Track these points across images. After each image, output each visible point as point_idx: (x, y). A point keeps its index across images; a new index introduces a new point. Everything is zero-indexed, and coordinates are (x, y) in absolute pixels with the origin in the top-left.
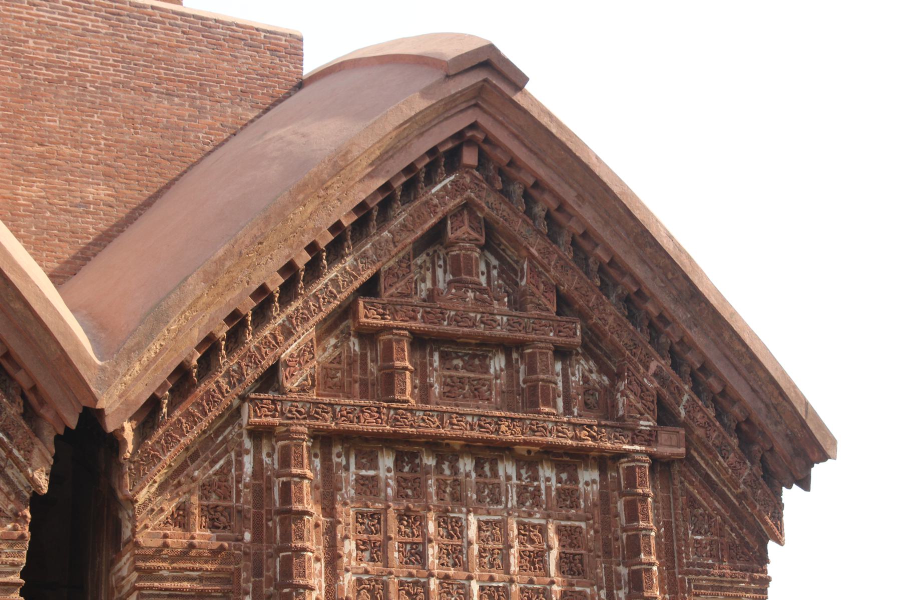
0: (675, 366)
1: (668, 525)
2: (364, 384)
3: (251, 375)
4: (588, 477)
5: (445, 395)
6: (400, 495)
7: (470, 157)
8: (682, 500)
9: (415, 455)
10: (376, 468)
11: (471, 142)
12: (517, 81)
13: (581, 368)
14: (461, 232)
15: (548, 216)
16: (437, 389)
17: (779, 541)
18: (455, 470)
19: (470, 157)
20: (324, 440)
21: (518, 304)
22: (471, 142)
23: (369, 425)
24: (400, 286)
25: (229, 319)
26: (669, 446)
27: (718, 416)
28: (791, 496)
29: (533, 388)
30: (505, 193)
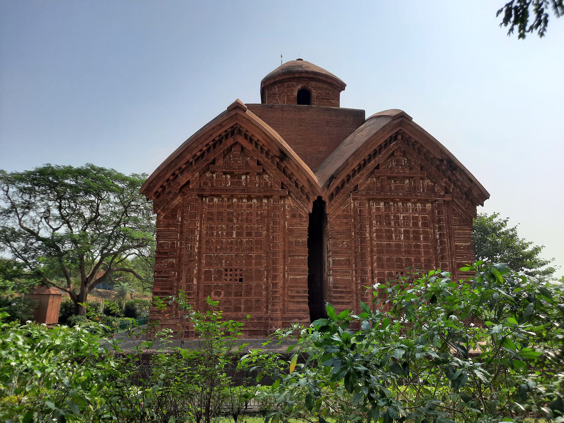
0: (449, 180)
1: (448, 216)
2: (377, 188)
4: (429, 205)
5: (395, 189)
6: (385, 211)
7: (399, 137)
8: (451, 209)
9: (388, 202)
11: (400, 134)
12: (410, 119)
13: (427, 182)
15: (418, 148)
18: (397, 205)
21: (411, 169)
22: (400, 134)
24: (384, 167)
25: (347, 176)
26: (448, 198)
27: (460, 191)
29: (415, 187)
30: (408, 144)
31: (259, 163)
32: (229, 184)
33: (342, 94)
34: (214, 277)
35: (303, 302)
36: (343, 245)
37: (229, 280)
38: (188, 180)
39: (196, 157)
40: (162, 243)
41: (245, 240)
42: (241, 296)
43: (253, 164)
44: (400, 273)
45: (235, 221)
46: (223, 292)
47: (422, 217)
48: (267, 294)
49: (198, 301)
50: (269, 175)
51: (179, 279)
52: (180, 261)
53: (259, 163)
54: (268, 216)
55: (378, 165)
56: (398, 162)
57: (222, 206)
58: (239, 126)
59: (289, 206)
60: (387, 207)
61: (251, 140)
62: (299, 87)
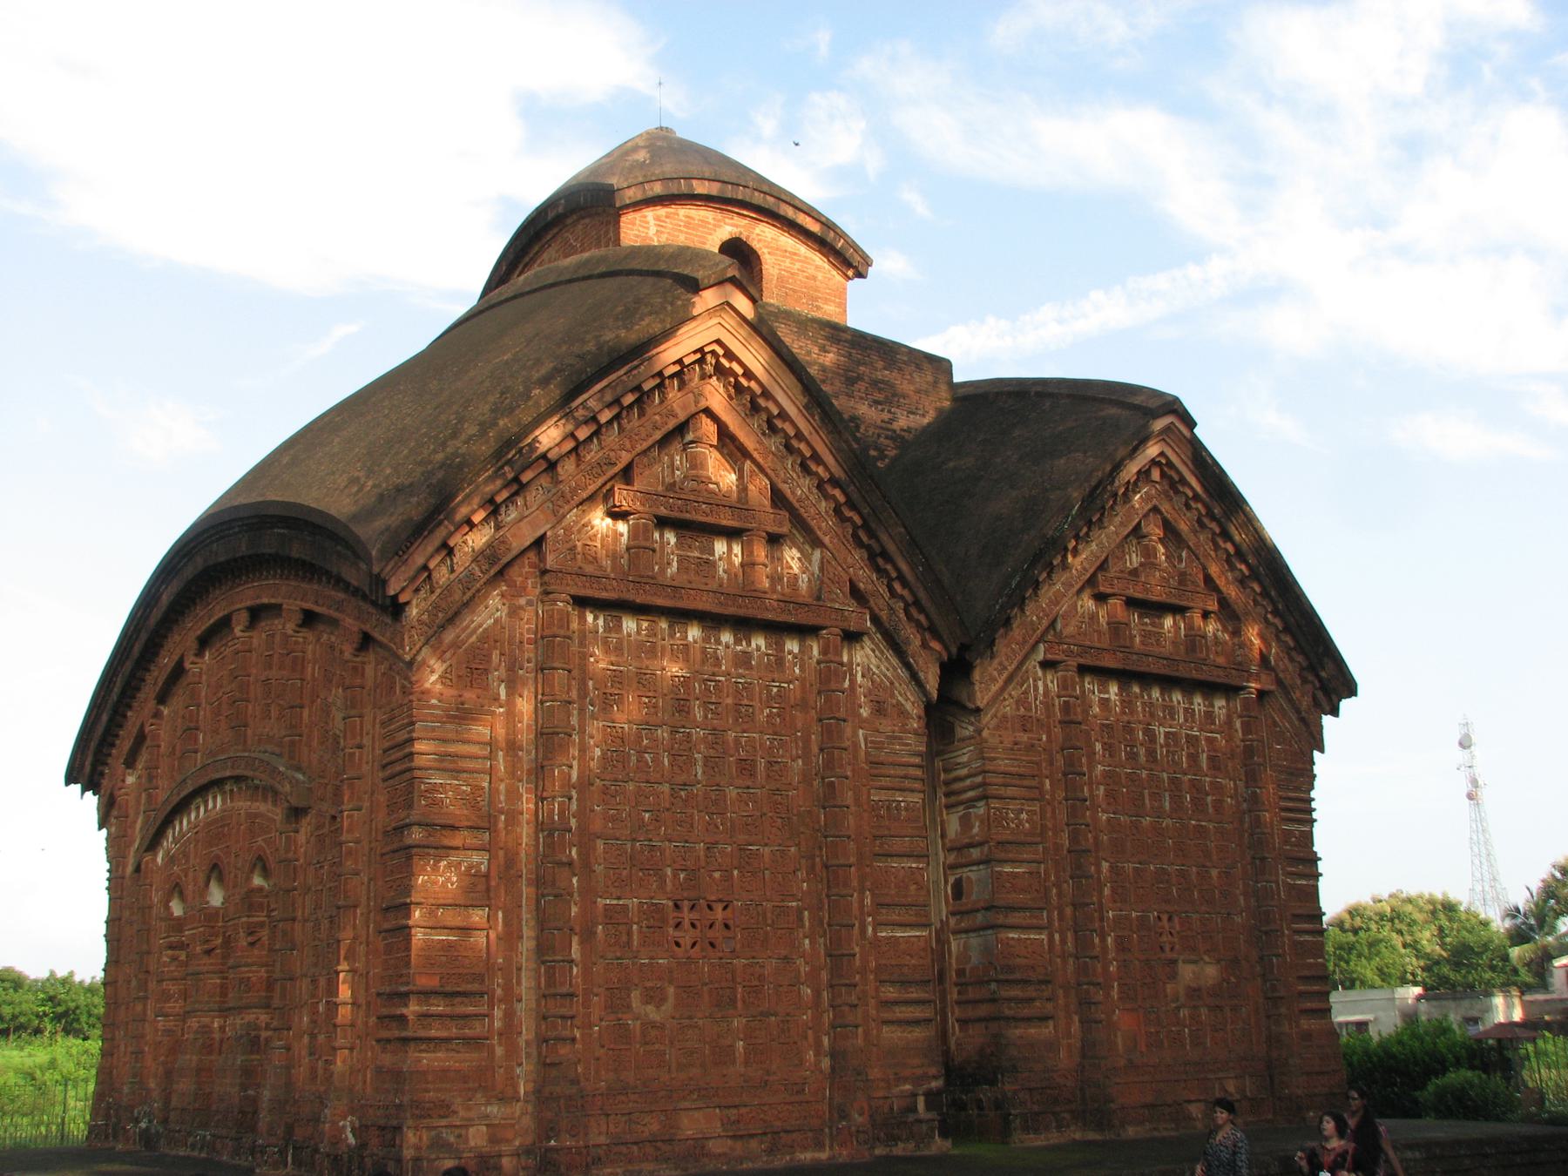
3: (1045, 623)
4: (1220, 703)
5: (1142, 643)
7: (1156, 474)
10: (1108, 692)
12: (1191, 424)
13: (1212, 627)
16: (1138, 639)
17: (1322, 750)
19: (1156, 474)
22: (1159, 464)
23: (1108, 662)
28: (1327, 720)
31: (778, 499)
32: (675, 564)
34: (640, 932)
35: (917, 1022)
36: (1021, 822)
37: (687, 941)
38: (541, 532)
39: (570, 445)
40: (434, 788)
41: (732, 792)
42: (733, 1001)
44: (1165, 917)
45: (699, 714)
46: (671, 990)
47: (1207, 739)
48: (817, 993)
49: (590, 1026)
50: (800, 550)
53: (778, 499)
54: (803, 705)
55: (1106, 559)
56: (1149, 553)
57: (652, 652)
58: (721, 352)
60: (1127, 703)
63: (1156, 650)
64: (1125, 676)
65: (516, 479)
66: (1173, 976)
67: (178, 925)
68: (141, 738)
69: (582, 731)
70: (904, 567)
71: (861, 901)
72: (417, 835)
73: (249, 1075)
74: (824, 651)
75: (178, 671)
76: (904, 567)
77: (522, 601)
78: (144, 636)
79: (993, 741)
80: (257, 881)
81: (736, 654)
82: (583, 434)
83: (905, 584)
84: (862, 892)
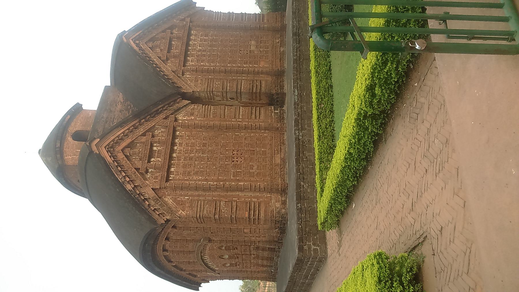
3: (173, 74)
7: (138, 42)
13: (175, 32)
14: (150, 45)
19: (138, 42)
20: (184, 66)
26: (188, 20)
31: (144, 135)
33: (84, 107)
35: (260, 111)
43: (144, 139)
48: (253, 132)
51: (239, 197)
52: (223, 197)
53: (144, 135)
56: (157, 46)
59: (184, 116)
61: (122, 139)
62: (70, 139)
63: (180, 47)
64: (186, 55)
65: (138, 194)
66: (253, 51)
67: (231, 265)
68: (190, 274)
69: (196, 181)
70: (160, 106)
71: (233, 121)
72: (217, 216)
73: (263, 249)
74: (179, 126)
75: (175, 266)
76: (160, 106)
77: (167, 193)
78: (167, 275)
79: (200, 89)
80: (224, 248)
81: (179, 146)
82: (128, 179)
83: (164, 106)
84: (232, 121)
